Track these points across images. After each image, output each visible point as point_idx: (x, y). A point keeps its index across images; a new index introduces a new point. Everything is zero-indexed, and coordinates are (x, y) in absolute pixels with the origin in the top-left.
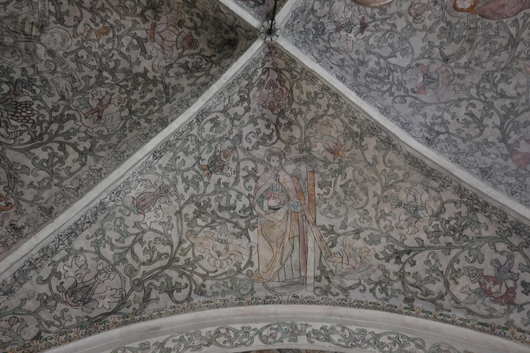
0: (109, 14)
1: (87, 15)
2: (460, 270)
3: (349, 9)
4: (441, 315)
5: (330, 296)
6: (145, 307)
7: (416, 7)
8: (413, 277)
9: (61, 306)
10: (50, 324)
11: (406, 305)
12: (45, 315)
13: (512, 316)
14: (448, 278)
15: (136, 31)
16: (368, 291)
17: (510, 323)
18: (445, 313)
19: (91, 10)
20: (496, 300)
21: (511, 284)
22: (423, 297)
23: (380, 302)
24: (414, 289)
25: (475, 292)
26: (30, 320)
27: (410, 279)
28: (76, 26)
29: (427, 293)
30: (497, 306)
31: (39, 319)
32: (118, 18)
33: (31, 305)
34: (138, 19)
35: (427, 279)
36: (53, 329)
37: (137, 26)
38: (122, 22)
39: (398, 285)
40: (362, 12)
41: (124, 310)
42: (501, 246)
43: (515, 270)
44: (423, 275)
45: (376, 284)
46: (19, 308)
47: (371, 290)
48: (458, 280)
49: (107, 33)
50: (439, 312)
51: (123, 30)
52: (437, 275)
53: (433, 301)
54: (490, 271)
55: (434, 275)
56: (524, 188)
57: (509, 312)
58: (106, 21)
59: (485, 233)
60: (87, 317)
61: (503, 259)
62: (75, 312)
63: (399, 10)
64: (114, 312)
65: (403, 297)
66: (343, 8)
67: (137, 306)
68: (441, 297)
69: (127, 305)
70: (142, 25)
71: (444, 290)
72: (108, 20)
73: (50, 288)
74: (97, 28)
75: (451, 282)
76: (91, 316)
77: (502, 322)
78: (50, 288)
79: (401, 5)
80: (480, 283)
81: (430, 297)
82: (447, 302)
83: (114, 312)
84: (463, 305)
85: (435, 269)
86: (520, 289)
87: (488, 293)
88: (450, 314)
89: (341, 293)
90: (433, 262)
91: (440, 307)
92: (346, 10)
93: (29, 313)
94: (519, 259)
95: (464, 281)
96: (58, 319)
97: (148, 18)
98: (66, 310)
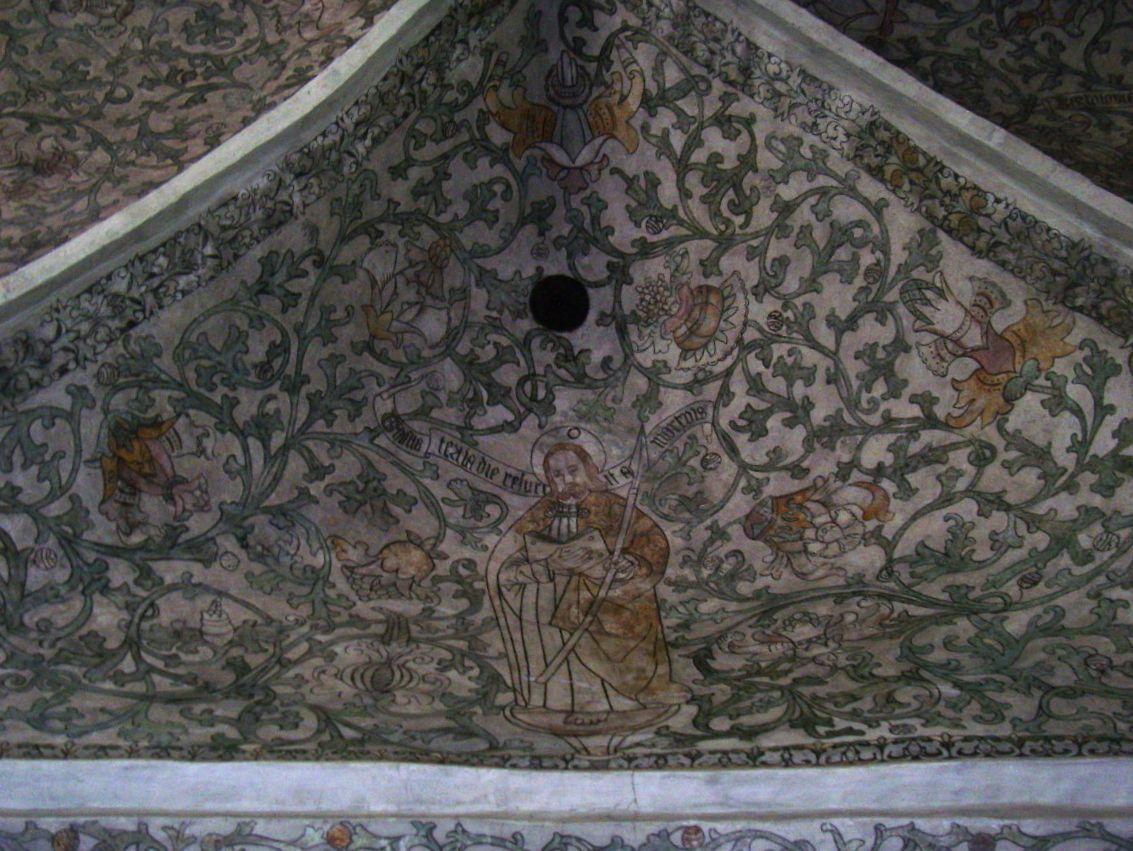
0: (1010, 61)
1: (1073, 57)
3: (307, 15)
7: (111, 10)
15: (936, 21)
19: (1061, 69)
28: (1105, 28)
32: (986, 54)
34: (928, 46)
37: (933, 33)
38: (975, 44)
40: (270, 13)
49: (1020, 17)
51: (976, 25)
58: (1021, 47)
63: (159, 10)
66: (326, 16)
70: (918, 33)
72: (1014, 48)
74: (1045, 29)
79: (154, 21)
92: (318, 13)
97: (901, 46)
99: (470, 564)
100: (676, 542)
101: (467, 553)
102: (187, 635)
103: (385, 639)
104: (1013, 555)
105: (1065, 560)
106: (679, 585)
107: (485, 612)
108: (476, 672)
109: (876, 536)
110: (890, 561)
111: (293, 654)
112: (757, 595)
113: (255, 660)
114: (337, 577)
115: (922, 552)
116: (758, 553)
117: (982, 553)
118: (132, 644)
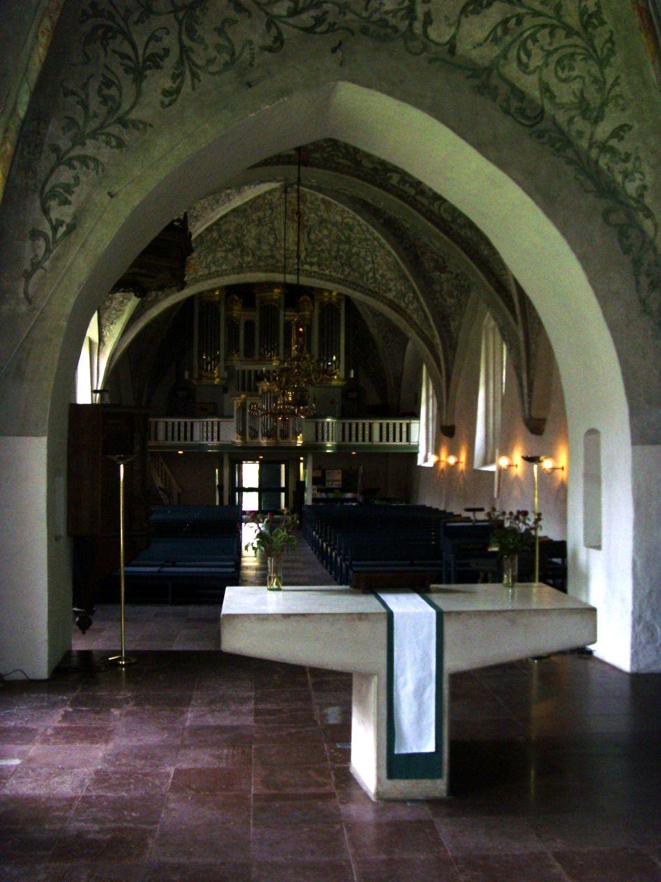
99: (271, 200)
100: (309, 198)
101: (270, 197)
102: (228, 232)
103: (258, 226)
104: (358, 236)
105: (364, 243)
106: (308, 208)
107: (274, 215)
108: (273, 236)
109: (342, 216)
110: (342, 222)
111: (245, 233)
112: (322, 216)
113: (239, 235)
114: (248, 209)
115: (347, 224)
116: (323, 208)
117: (355, 231)
118: (220, 237)
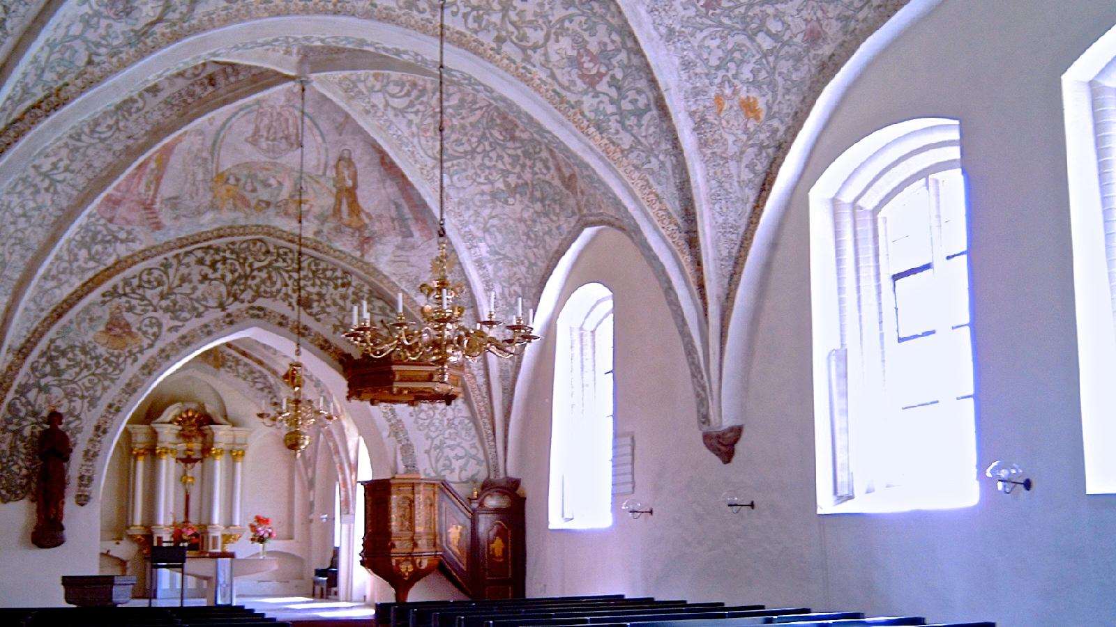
2: (568, 29)
4: (524, 68)
5: (415, 13)
6: (193, 10)
8: (517, 14)
9: (104, 22)
10: (98, 45)
11: (494, 45)
12: (91, 35)
13: (584, 98)
14: (553, 31)
16: (460, 15)
17: (579, 103)
18: (529, 67)
20: (582, 76)
21: (603, 70)
22: (516, 41)
23: (468, 33)
24: (511, 28)
25: (569, 58)
26: (78, 44)
27: (513, 15)
29: (523, 38)
30: (579, 82)
31: (85, 41)
33: (76, 30)
35: (531, 22)
36: (103, 50)
39: (496, 18)
41: (173, 16)
42: (615, 37)
43: (614, 62)
44: (529, 17)
45: (474, 8)
46: (66, 35)
47: (465, 16)
48: (560, 38)
50: (524, 64)
52: (544, 23)
53: (524, 49)
54: (593, 47)
55: (541, 21)
56: (667, 8)
57: (586, 92)
59: (608, 17)
60: (133, 31)
61: (610, 47)
62: (120, 27)
64: (160, 20)
65: (495, 34)
67: (184, 9)
68: (535, 48)
69: (172, 8)
71: (541, 42)
73: (91, 7)
75: (553, 37)
76: (137, 28)
77: (572, 98)
78: (91, 7)
80: (579, 53)
81: (523, 43)
82: (537, 57)
83: (160, 20)
84: (550, 66)
85: (544, 16)
86: (607, 79)
87: (580, 65)
88: (534, 69)
89: (428, 10)
90: (547, 7)
91: (527, 59)
93: (76, 38)
94: (623, 56)
95: (565, 43)
96: (103, 38)
98: (109, 26)
